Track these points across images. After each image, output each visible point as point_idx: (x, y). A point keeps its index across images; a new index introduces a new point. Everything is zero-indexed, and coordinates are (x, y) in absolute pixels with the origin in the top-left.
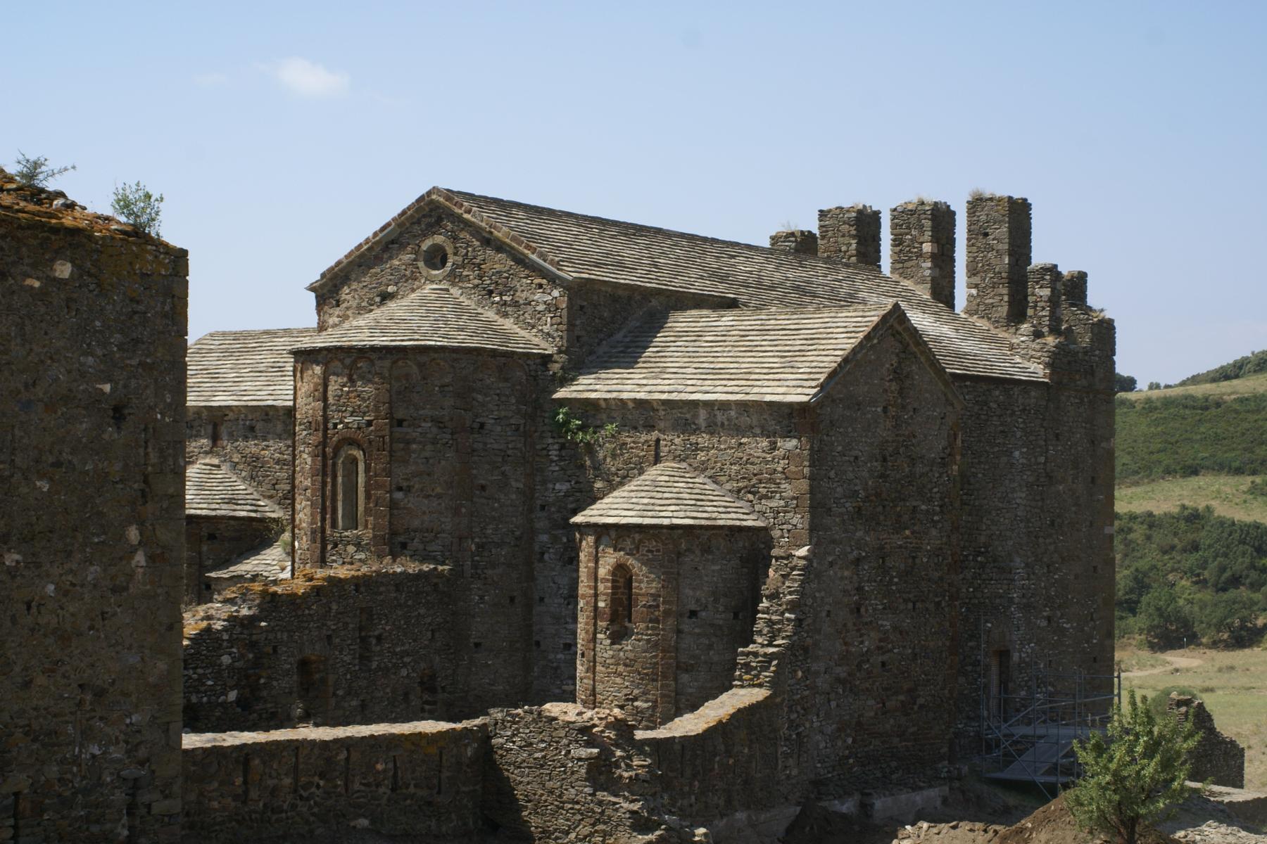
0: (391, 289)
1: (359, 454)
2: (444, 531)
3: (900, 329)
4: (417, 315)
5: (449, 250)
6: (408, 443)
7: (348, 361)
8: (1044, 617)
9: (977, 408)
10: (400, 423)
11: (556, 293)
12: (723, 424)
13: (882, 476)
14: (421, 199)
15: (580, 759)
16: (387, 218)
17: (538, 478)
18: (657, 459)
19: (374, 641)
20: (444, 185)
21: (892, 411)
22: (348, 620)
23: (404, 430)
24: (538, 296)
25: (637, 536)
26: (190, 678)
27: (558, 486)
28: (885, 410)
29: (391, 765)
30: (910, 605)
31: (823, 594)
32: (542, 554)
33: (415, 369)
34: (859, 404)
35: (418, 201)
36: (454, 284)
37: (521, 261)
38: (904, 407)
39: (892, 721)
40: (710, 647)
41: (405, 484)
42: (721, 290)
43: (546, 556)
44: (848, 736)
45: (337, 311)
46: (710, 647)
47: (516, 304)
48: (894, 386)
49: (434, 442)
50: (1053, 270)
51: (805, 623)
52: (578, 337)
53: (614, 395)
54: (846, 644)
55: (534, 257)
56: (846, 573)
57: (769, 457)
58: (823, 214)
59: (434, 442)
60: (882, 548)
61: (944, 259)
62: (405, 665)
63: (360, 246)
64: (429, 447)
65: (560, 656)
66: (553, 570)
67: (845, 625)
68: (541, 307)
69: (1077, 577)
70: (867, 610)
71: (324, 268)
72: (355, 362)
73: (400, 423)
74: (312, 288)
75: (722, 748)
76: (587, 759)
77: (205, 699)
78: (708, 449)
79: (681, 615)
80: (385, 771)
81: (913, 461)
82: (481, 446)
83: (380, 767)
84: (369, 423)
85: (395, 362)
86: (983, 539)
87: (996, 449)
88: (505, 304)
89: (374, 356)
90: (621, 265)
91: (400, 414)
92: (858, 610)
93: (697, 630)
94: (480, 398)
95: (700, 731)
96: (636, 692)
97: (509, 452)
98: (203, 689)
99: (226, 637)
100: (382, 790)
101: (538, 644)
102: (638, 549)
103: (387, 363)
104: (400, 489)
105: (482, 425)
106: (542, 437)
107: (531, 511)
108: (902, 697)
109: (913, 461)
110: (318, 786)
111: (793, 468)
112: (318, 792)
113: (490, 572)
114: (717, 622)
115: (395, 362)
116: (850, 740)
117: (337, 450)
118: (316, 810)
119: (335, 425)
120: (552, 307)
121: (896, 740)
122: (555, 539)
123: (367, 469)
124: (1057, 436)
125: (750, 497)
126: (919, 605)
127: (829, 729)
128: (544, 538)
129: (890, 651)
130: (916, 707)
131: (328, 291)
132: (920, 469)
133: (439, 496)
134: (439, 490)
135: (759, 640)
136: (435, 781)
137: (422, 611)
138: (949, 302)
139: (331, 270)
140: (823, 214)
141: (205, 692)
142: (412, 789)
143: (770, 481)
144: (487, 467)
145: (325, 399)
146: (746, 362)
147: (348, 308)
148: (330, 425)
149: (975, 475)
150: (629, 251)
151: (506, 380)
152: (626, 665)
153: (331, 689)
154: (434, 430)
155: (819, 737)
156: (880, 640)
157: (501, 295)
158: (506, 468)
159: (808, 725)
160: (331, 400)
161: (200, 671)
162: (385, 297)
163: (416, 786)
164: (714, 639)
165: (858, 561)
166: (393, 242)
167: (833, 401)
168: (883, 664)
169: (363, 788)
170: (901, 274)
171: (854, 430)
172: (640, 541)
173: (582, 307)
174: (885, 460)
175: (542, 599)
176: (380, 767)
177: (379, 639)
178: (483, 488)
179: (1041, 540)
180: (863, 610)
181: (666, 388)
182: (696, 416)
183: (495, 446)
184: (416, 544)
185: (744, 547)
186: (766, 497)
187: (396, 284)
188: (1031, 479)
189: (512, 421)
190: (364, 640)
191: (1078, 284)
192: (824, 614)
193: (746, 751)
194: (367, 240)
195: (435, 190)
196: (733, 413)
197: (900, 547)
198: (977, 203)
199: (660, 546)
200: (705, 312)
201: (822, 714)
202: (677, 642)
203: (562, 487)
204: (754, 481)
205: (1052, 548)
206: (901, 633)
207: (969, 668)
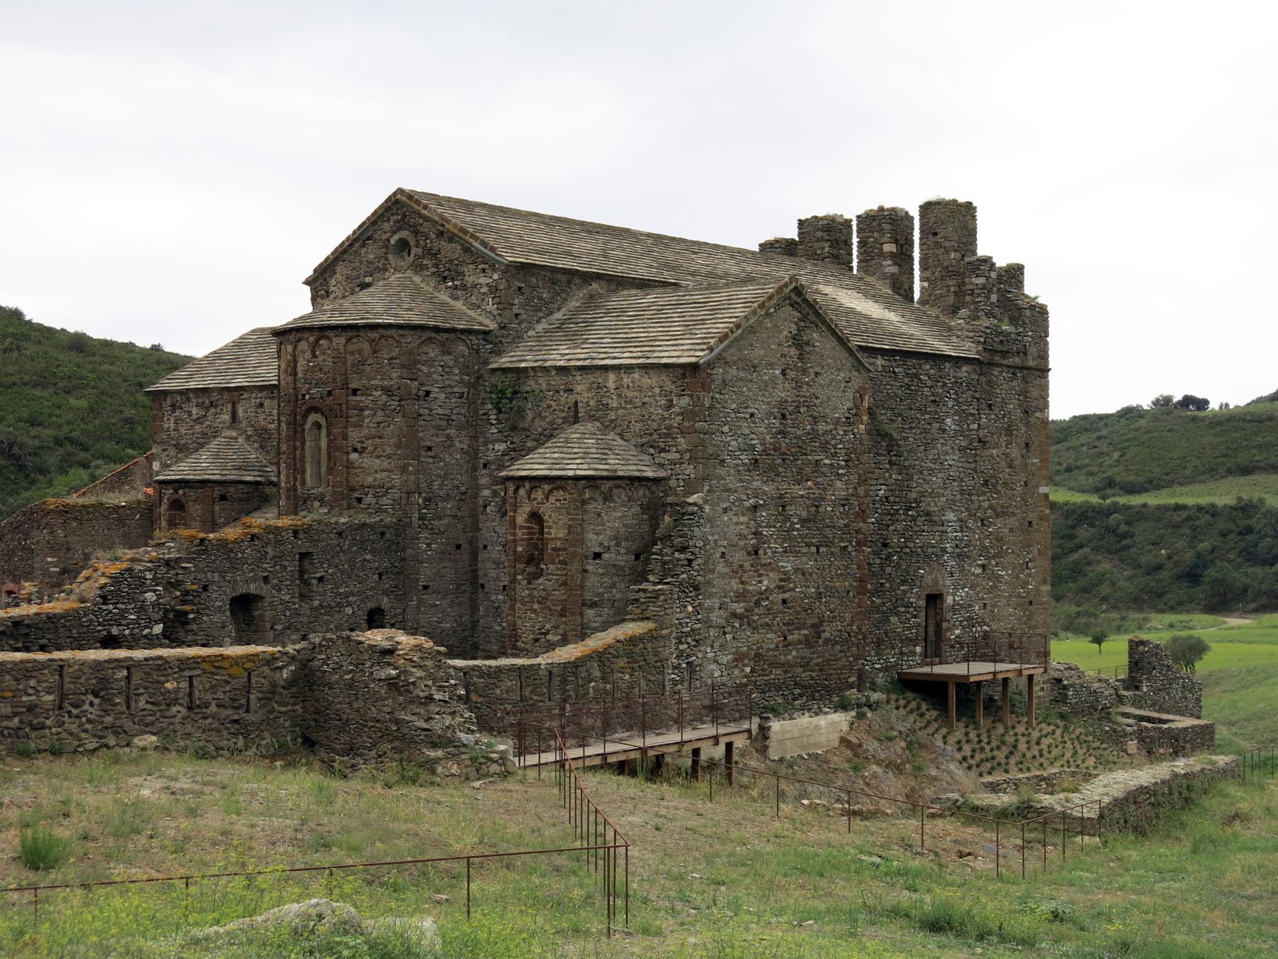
0: (368, 280)
1: (323, 421)
2: (393, 487)
3: (798, 300)
4: (389, 300)
5: (412, 243)
6: (362, 410)
7: (311, 339)
9: (906, 380)
10: (355, 392)
11: (496, 276)
12: (628, 387)
13: (781, 432)
14: (389, 198)
15: (380, 680)
16: (364, 218)
17: (481, 440)
18: (576, 420)
19: (314, 582)
20: (407, 187)
21: (792, 374)
22: (286, 563)
23: (358, 398)
24: (483, 280)
25: (547, 487)
26: (110, 612)
27: (497, 447)
28: (784, 373)
29: (185, 685)
30: (814, 549)
31: (716, 537)
32: (485, 507)
33: (366, 346)
34: (755, 367)
35: (386, 201)
36: (416, 272)
37: (467, 250)
38: (804, 371)
39: (794, 653)
40: (613, 586)
41: (359, 446)
42: (668, 276)
43: (488, 509)
44: (746, 665)
46: (613, 586)
47: (464, 288)
48: (793, 351)
49: (384, 408)
50: (987, 261)
51: (694, 564)
52: (517, 315)
53: (540, 363)
54: (742, 583)
55: (476, 244)
56: (742, 519)
57: (666, 414)
58: (801, 223)
59: (384, 408)
60: (781, 497)
61: (903, 257)
62: (349, 605)
64: (380, 413)
65: (500, 597)
66: (493, 520)
67: (741, 566)
68: (484, 290)
69: (1011, 530)
70: (766, 553)
71: (316, 265)
72: (317, 341)
73: (355, 392)
74: (307, 282)
75: (598, 674)
76: (385, 680)
77: (127, 632)
78: (617, 409)
79: (586, 558)
80: (177, 690)
81: (815, 420)
82: (427, 411)
83: (168, 685)
84: (330, 393)
85: (349, 340)
86: (914, 495)
87: (927, 416)
88: (456, 288)
89: (331, 334)
90: (569, 254)
91: (353, 386)
92: (756, 553)
93: (601, 571)
94: (425, 369)
95: (573, 659)
96: (548, 626)
97: (453, 417)
98: (123, 622)
99: (149, 576)
100: (174, 709)
101: (483, 586)
102: (547, 499)
103: (342, 340)
104: (355, 450)
105: (428, 393)
106: (483, 404)
107: (475, 469)
108: (806, 632)
109: (815, 420)
110: (92, 704)
111: (686, 424)
112: (91, 710)
113: (436, 523)
114: (618, 563)
115: (349, 340)
116: (748, 670)
117: (305, 416)
118: (88, 726)
119: (304, 396)
120: (494, 289)
121: (799, 670)
122: (495, 493)
124: (990, 406)
125: (652, 450)
126: (822, 549)
127: (724, 660)
128: (486, 493)
130: (821, 641)
131: (320, 281)
132: (822, 427)
133: (389, 457)
134: (389, 451)
135: (651, 578)
136: (243, 701)
137: (368, 557)
138: (909, 296)
139: (321, 265)
140: (801, 223)
141: (128, 625)
142: (213, 708)
143: (667, 435)
144: (433, 431)
145: (295, 374)
146: (655, 331)
148: (300, 397)
149: (906, 439)
150: (584, 245)
151: (450, 353)
152: (539, 602)
153: (268, 625)
154: (384, 398)
155: (713, 667)
156: (781, 580)
157: (453, 280)
158: (452, 432)
159: (700, 655)
160: (300, 375)
161: (120, 606)
162: (364, 286)
163: (218, 706)
164: (616, 579)
165: (755, 508)
167: (726, 363)
169: (149, 706)
170: (865, 272)
171: (749, 390)
172: (551, 491)
173: (520, 288)
174: (784, 416)
175: (485, 547)
176: (168, 685)
177: (321, 579)
178: (429, 449)
179: (974, 498)
180: (761, 552)
181: (583, 356)
182: (606, 380)
183: (440, 411)
184: (370, 499)
185: (644, 496)
186: (662, 450)
188: (964, 444)
189: (456, 390)
190: (306, 583)
191: (1014, 274)
192: (718, 555)
193: (627, 677)
195: (400, 191)
196: (636, 376)
197: (802, 496)
198: (926, 208)
199: (568, 496)
200: (634, 292)
201: (717, 645)
202: (582, 581)
203: (501, 447)
204: (655, 436)
205: (986, 504)
206: (803, 574)
207: (902, 609)
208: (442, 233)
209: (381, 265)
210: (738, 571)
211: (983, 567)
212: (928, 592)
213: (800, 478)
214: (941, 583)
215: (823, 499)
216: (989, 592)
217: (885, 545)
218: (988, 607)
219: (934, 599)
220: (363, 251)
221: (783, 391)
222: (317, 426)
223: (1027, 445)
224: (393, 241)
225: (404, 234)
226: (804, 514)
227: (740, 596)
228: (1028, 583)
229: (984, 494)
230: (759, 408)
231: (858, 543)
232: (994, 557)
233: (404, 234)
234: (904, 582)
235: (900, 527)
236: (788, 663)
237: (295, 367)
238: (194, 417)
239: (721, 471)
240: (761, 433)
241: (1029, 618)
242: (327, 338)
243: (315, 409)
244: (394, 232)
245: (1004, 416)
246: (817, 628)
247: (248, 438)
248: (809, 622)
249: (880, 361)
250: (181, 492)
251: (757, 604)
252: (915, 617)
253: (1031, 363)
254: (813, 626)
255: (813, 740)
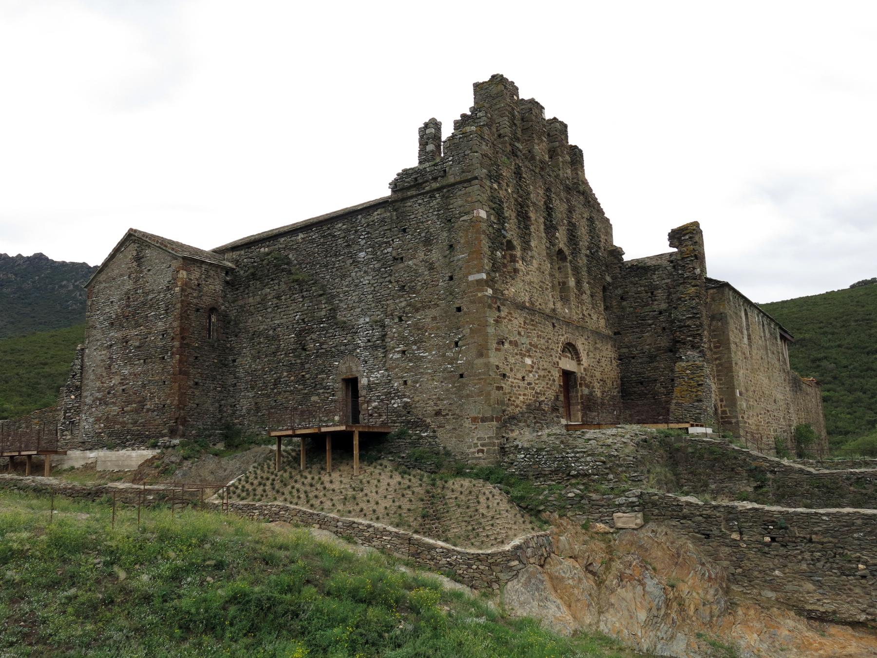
8: (398, 352)
30: (142, 361)
69: (434, 318)
129: (127, 384)
168: (123, 390)
207: (321, 391)
210: (100, 377)
211: (404, 352)
212: (344, 376)
213: (137, 325)
214: (354, 369)
215: (150, 333)
216: (410, 370)
217: (305, 350)
218: (409, 382)
219: (352, 383)
221: (129, 285)
223: (451, 246)
226: (137, 344)
227: (99, 390)
228: (457, 359)
229: (402, 296)
230: (115, 299)
231: (172, 354)
232: (415, 343)
234: (323, 372)
235: (314, 336)
236: (124, 422)
239: (94, 332)
240: (114, 310)
241: (460, 389)
245: (419, 234)
246: (142, 403)
248: (137, 400)
249: (301, 236)
251: (109, 393)
252: (333, 395)
253: (451, 180)
254: (139, 402)
255: (126, 463)
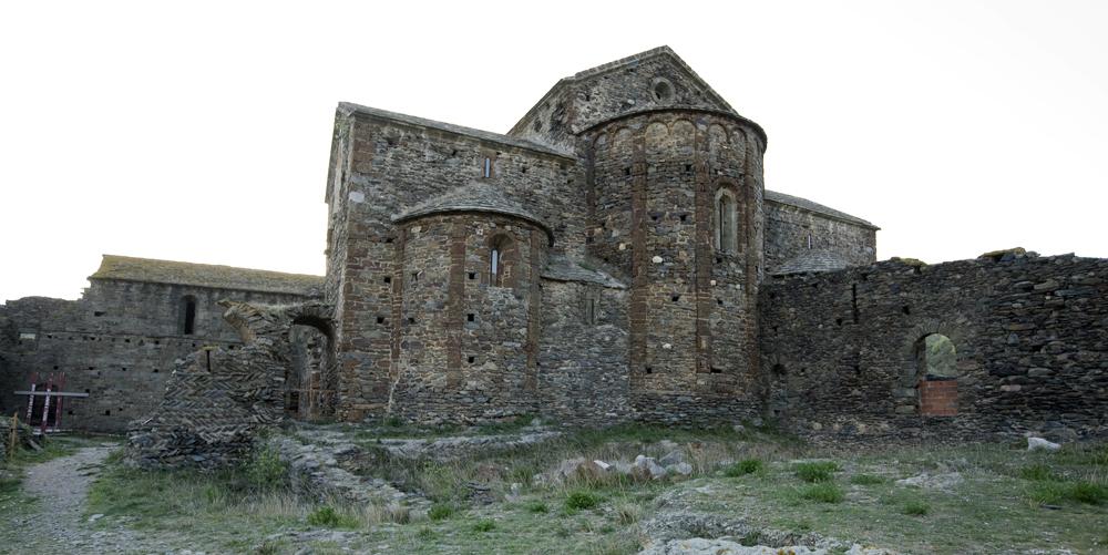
0: (630, 101)
5: (673, 89)
45: (588, 104)
63: (610, 64)
123: (739, 209)
147: (596, 104)
160: (713, 152)
166: (632, 70)
187: (634, 99)
194: (616, 62)
208: (698, 93)
209: (644, 95)
220: (627, 78)
222: (724, 199)
224: (658, 80)
225: (666, 81)
233: (666, 81)
237: (708, 145)
238: (427, 159)
242: (741, 130)
243: (726, 185)
244: (656, 76)
247: (508, 196)
250: (508, 228)
